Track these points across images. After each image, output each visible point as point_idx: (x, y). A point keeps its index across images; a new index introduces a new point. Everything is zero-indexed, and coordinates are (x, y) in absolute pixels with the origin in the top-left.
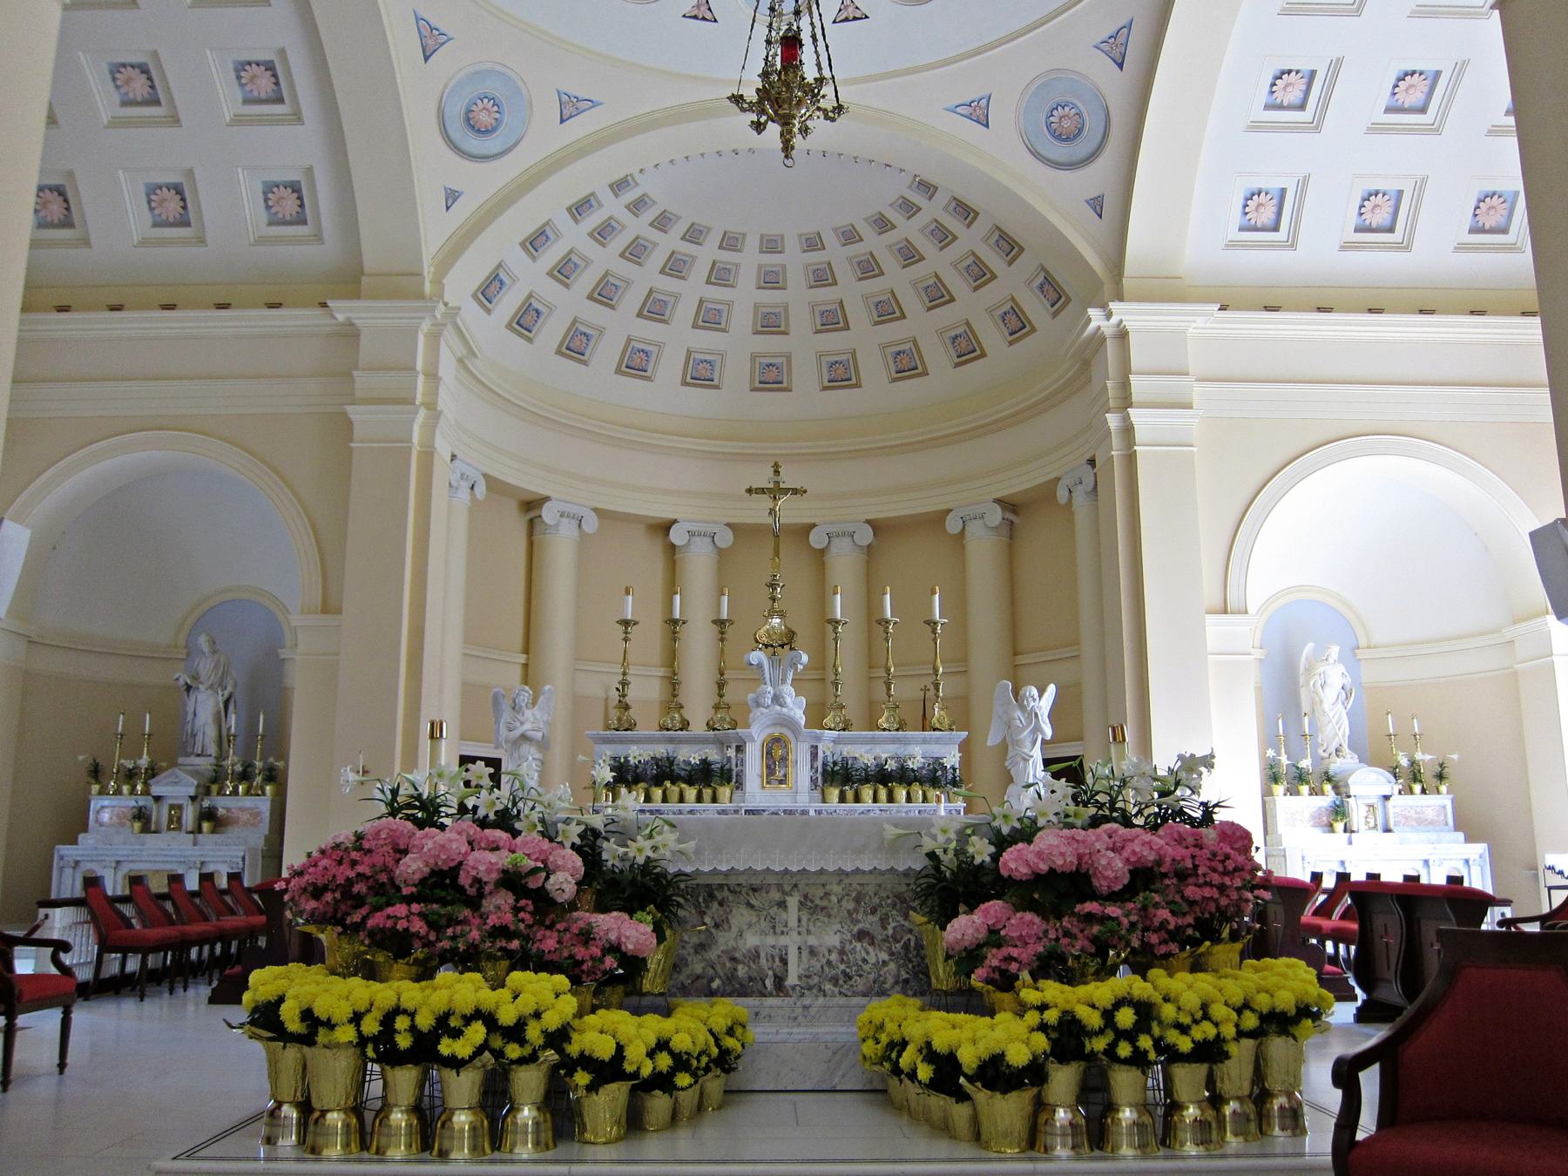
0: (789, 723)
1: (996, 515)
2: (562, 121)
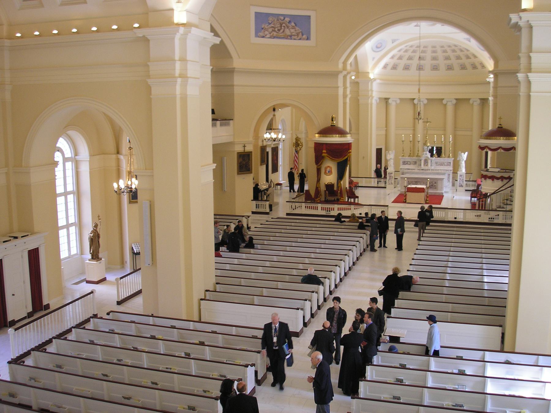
0: (427, 157)
1: (479, 101)
2: (393, 43)
